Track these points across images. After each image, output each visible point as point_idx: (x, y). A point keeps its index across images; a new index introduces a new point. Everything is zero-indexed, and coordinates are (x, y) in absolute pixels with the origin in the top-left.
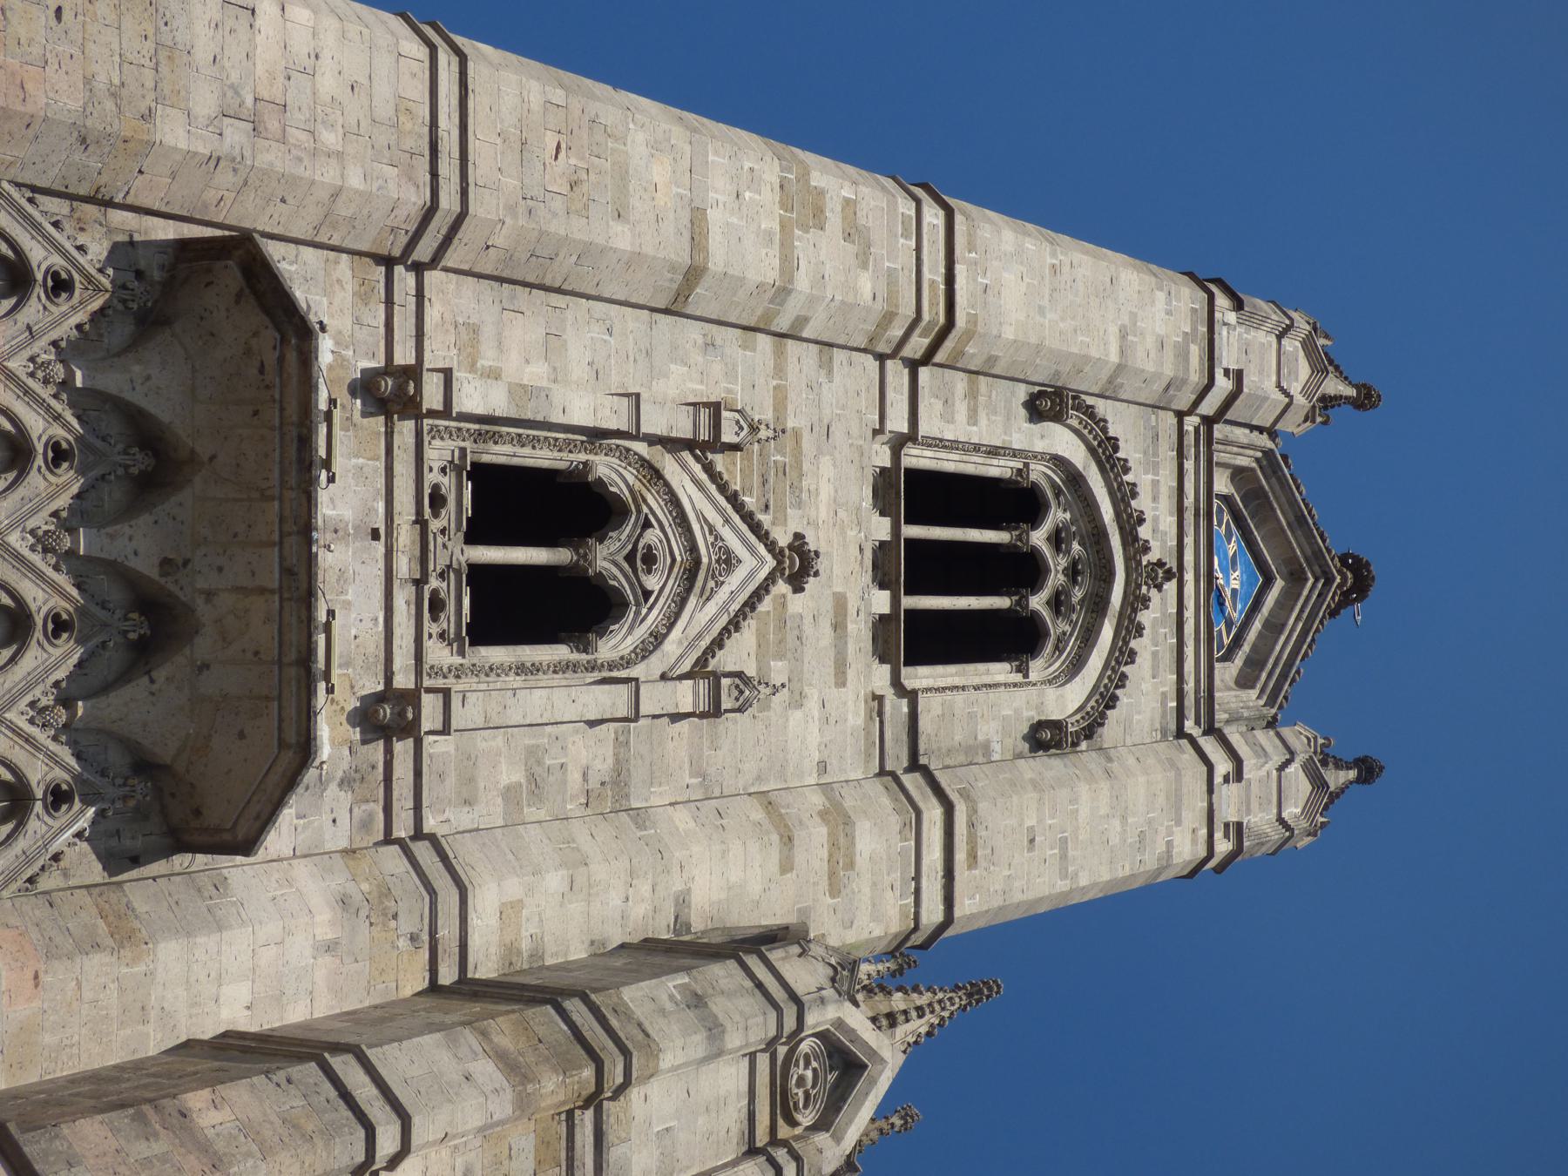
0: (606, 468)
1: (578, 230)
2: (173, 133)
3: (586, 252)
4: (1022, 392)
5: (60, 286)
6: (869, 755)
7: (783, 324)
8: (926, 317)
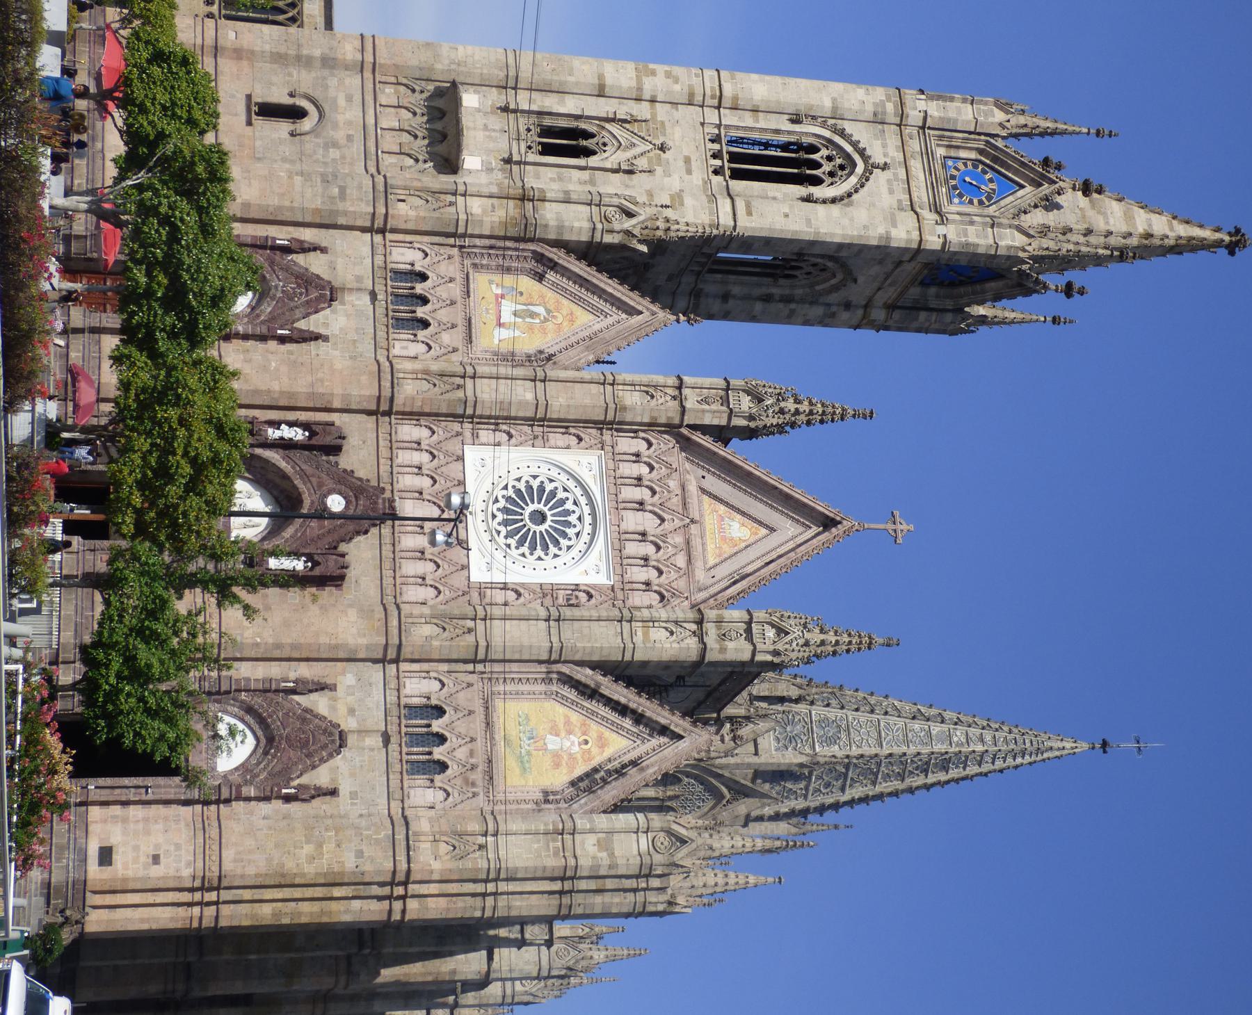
0: (583, 125)
1: (555, 78)
2: (439, 66)
3: (561, 83)
4: (787, 117)
5: (422, 92)
6: (705, 190)
7: (647, 96)
8: (708, 92)
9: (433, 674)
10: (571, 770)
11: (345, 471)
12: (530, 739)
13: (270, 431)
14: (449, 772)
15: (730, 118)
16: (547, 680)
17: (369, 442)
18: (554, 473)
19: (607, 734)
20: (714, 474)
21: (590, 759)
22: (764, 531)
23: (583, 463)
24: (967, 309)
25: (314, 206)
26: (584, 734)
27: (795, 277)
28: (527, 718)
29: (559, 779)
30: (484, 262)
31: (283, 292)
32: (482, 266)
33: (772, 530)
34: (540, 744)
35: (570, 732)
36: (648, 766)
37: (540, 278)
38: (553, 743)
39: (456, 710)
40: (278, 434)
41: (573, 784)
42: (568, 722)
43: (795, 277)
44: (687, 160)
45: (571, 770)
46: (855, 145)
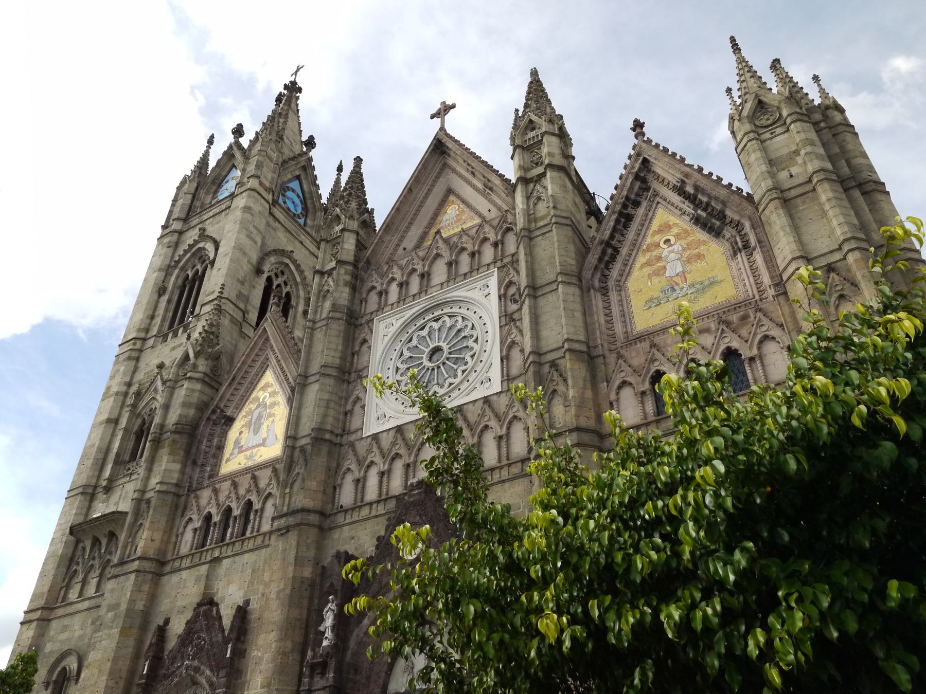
9: (613, 397)
10: (699, 243)
11: (377, 547)
12: (673, 289)
13: (325, 643)
14: (735, 344)
15: (154, 331)
16: (605, 291)
17: (353, 533)
18: (395, 355)
19: (655, 226)
20: (401, 240)
21: (686, 231)
22: (452, 198)
23: (385, 331)
24: (324, 200)
25: (117, 636)
26: (658, 245)
27: (288, 294)
28: (651, 300)
29: (715, 251)
30: (208, 469)
31: (193, 659)
32: (211, 470)
33: (450, 191)
34: (678, 280)
35: (659, 258)
36: (682, 173)
37: (230, 421)
38: (674, 268)
39: (653, 360)
40: (329, 634)
41: (716, 233)
42: (648, 264)
43: (288, 294)
44: (173, 349)
45: (699, 243)
46: (186, 252)
